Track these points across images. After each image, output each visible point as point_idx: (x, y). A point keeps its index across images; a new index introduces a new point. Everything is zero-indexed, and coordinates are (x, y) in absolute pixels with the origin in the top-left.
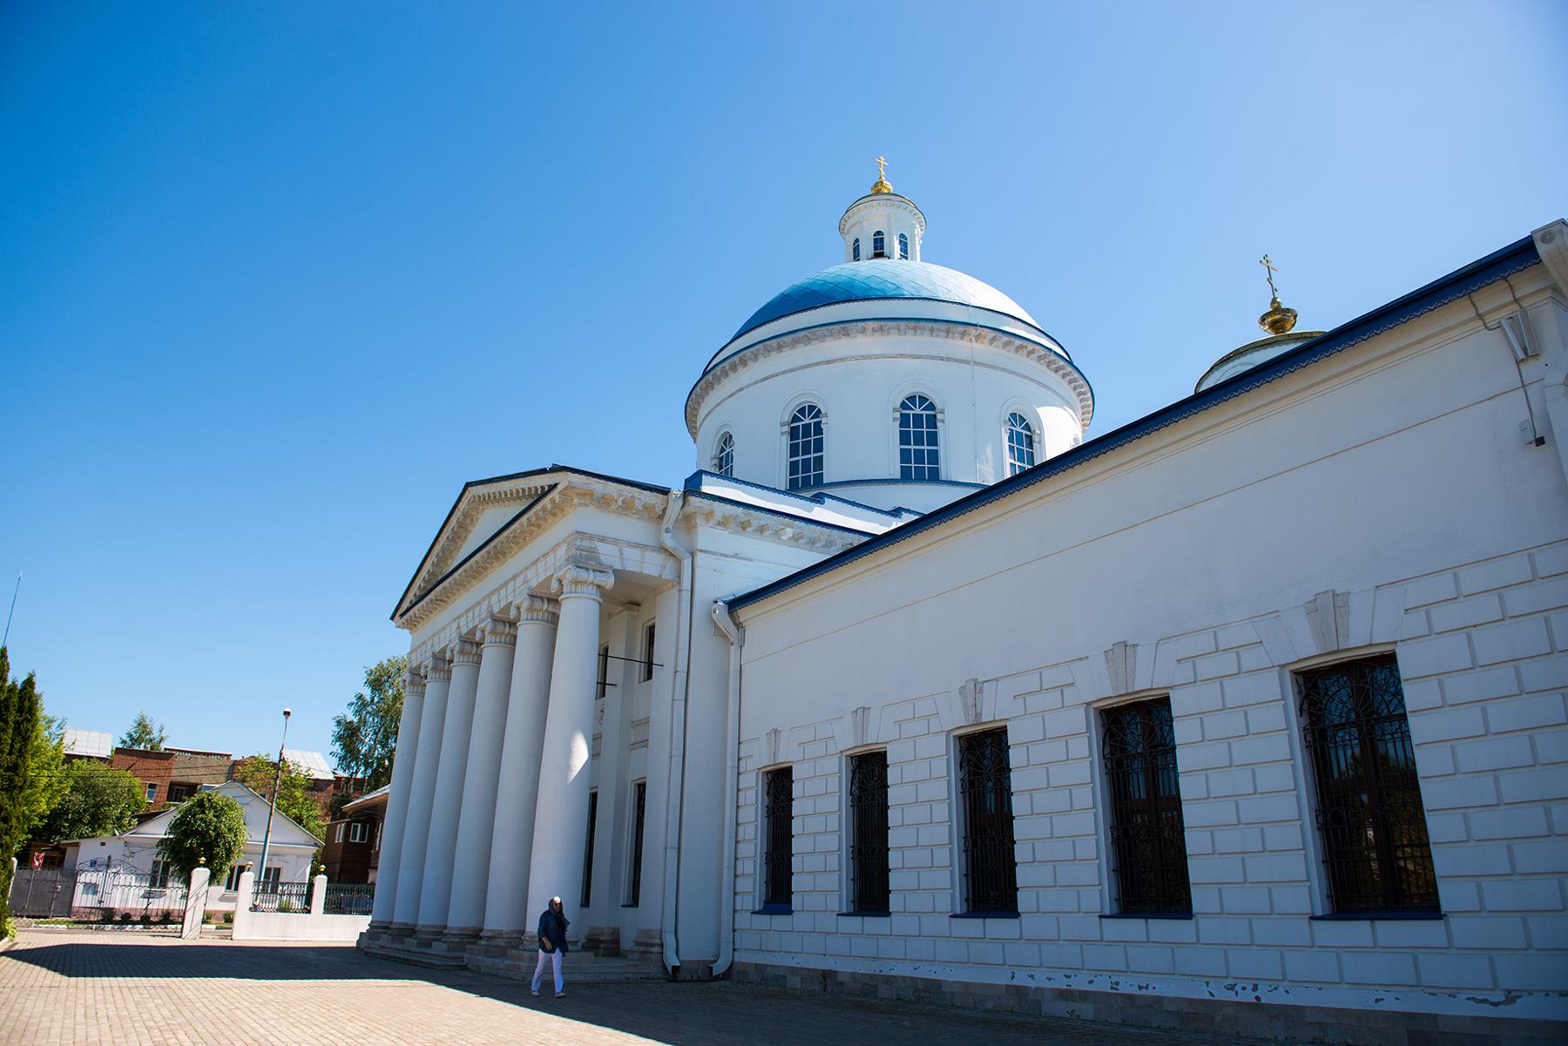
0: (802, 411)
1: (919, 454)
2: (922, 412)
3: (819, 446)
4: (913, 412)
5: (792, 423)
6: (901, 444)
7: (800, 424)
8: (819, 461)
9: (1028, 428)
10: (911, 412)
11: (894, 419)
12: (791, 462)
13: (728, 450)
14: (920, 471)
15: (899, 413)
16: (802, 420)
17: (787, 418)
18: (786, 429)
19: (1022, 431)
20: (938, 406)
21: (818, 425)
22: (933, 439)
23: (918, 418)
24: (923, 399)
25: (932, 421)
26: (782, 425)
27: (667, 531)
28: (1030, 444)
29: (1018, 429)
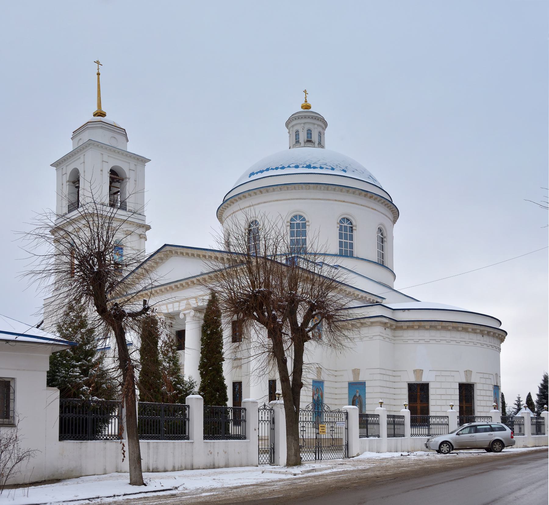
0: (295, 216)
1: (346, 243)
2: (347, 225)
7: (295, 222)
10: (343, 225)
14: (346, 251)
18: (289, 224)
20: (354, 223)
23: (346, 227)
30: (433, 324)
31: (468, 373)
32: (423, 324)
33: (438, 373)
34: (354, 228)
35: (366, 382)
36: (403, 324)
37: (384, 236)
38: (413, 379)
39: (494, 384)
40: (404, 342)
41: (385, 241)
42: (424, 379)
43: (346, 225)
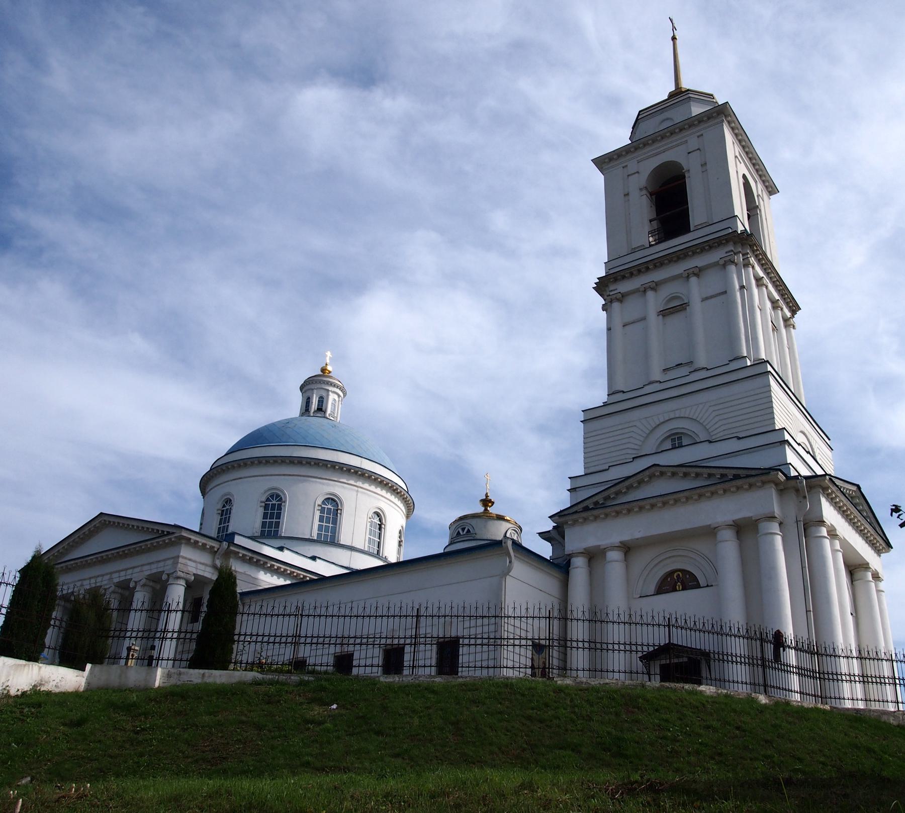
0: (272, 496)
3: (279, 516)
5: (266, 501)
6: (319, 522)
7: (271, 503)
8: (278, 524)
9: (380, 520)
10: (326, 507)
12: (263, 522)
13: (227, 507)
17: (264, 499)
21: (280, 505)
23: (329, 509)
26: (262, 502)
29: (375, 521)
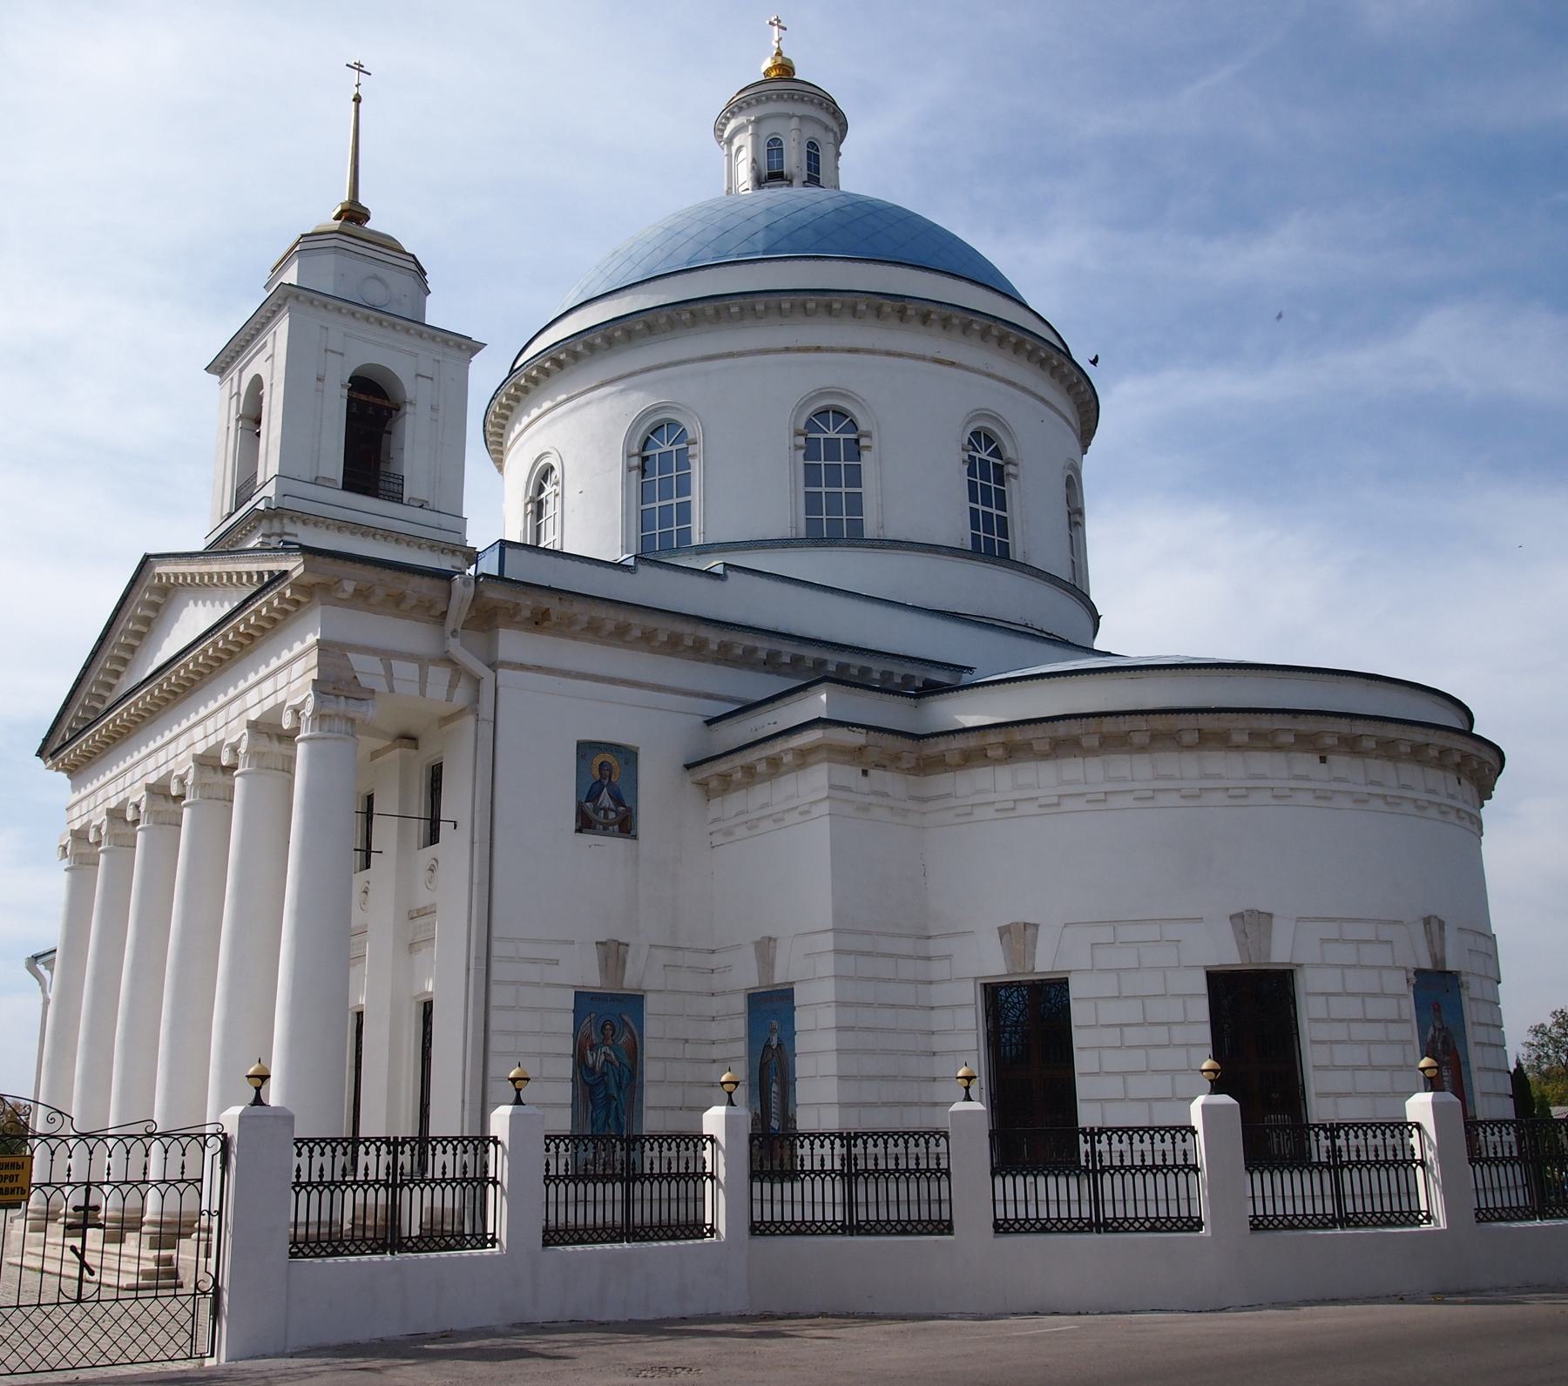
0: (656, 429)
2: (837, 436)
4: (826, 436)
7: (657, 452)
9: (997, 453)
10: (822, 436)
11: (797, 448)
15: (803, 438)
16: (661, 447)
18: (636, 461)
19: (989, 458)
20: (863, 426)
22: (855, 477)
24: (841, 414)
25: (855, 449)
27: (454, 633)
28: (1000, 480)
29: (984, 456)
30: (1062, 729)
31: (1251, 922)
32: (1018, 735)
33: (1104, 935)
34: (863, 442)
35: (796, 988)
36: (942, 745)
37: (1004, 458)
38: (996, 966)
39: (1412, 964)
40: (957, 815)
41: (1008, 474)
42: (1044, 964)
43: (832, 434)
